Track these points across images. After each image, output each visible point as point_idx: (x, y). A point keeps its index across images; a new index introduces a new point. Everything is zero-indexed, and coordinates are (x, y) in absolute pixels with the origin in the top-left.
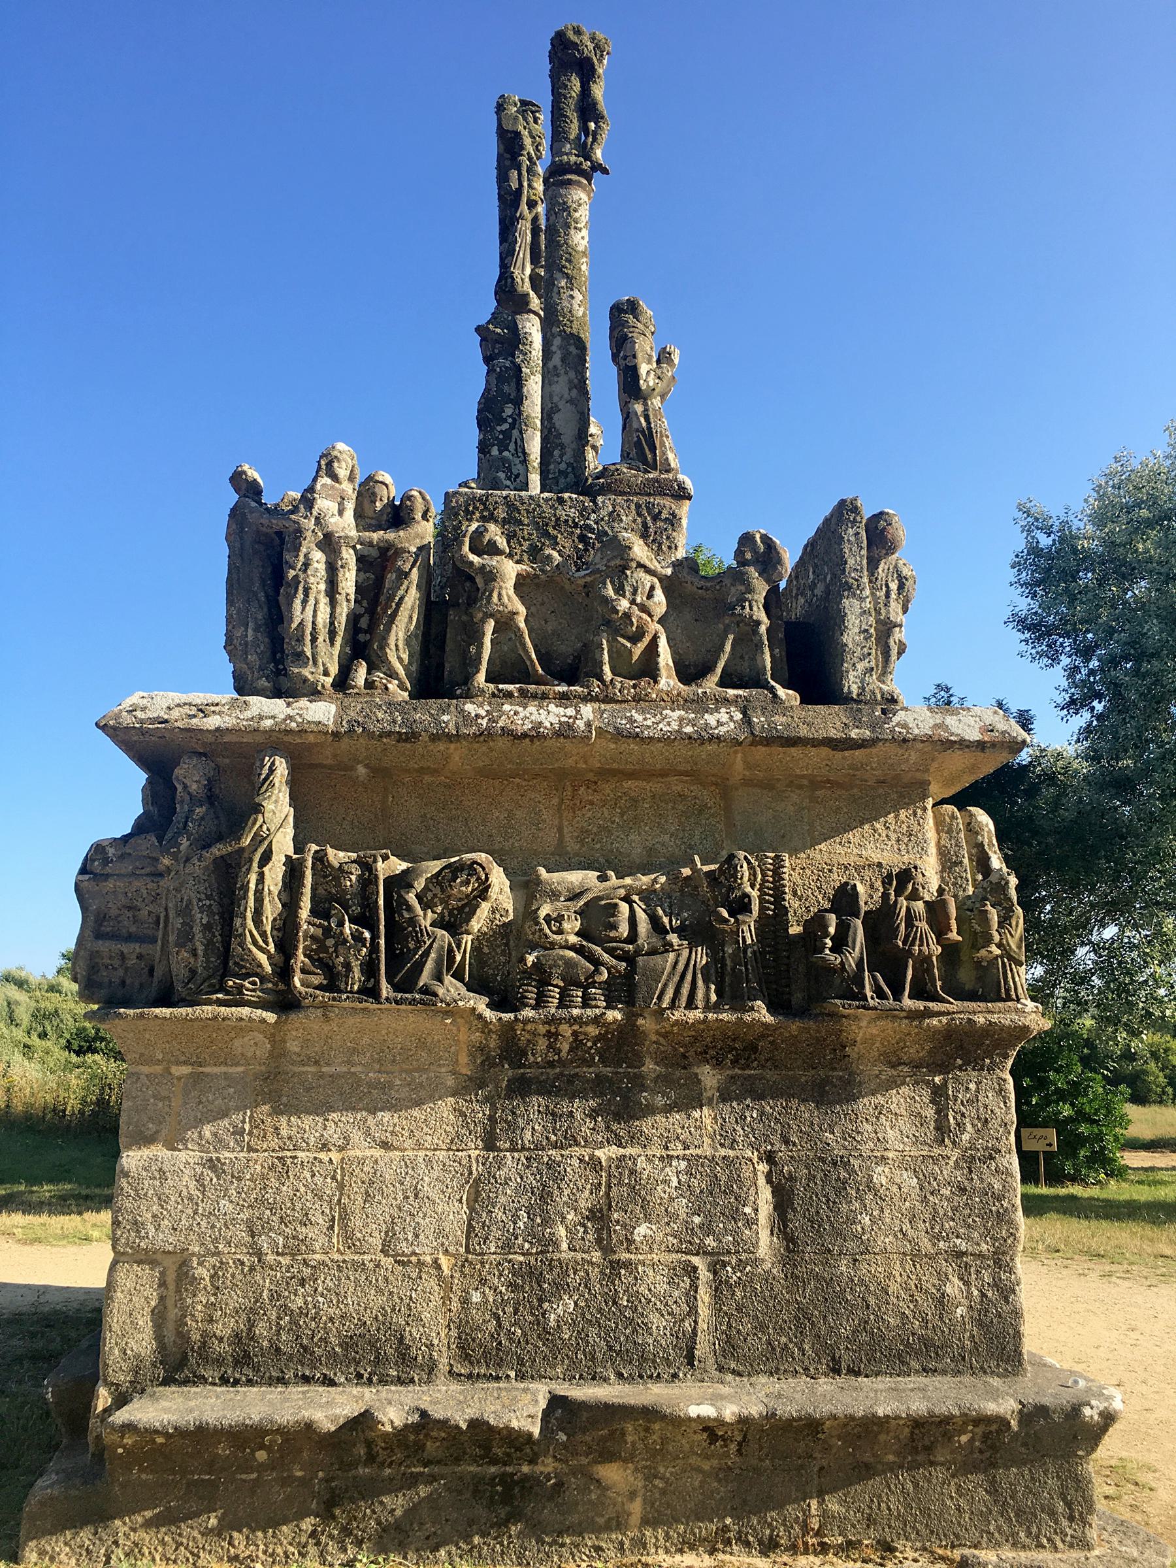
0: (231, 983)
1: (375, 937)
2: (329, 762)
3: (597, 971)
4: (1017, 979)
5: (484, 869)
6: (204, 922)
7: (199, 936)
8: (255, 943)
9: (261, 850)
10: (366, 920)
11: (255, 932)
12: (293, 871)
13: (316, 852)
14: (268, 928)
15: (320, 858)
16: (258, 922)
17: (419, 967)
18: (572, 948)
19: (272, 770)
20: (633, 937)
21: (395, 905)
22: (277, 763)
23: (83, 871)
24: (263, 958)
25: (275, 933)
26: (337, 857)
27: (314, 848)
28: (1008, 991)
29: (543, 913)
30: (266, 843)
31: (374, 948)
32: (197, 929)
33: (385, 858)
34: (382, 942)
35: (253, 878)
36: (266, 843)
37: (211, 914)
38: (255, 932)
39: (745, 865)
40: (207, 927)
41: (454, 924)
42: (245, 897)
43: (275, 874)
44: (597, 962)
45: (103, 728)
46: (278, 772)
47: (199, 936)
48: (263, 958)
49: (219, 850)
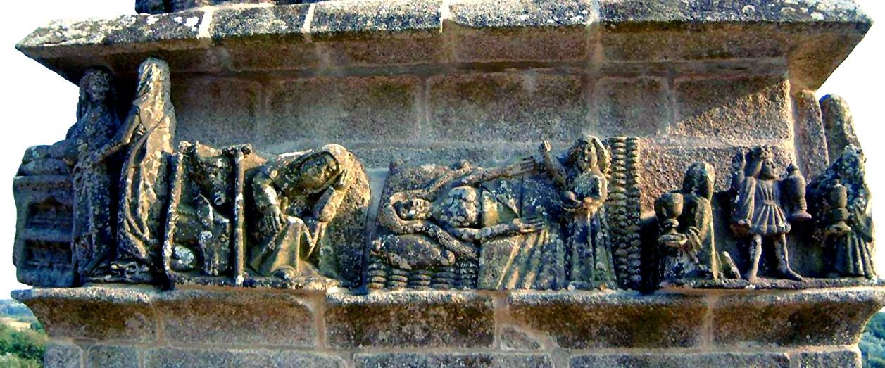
0: (114, 267)
1: (234, 224)
2: (214, 69)
3: (445, 255)
4: (866, 255)
5: (335, 159)
6: (96, 213)
7: (92, 225)
8: (133, 231)
9: (138, 147)
10: (226, 209)
11: (132, 220)
12: (169, 165)
13: (189, 148)
14: (145, 218)
15: (191, 154)
16: (134, 212)
17: (272, 254)
18: (423, 233)
19: (149, 76)
20: (479, 223)
21: (252, 192)
22: (154, 69)
23: (20, 173)
24: (140, 246)
25: (152, 222)
26: (206, 152)
27: (185, 144)
28: (856, 268)
29: (393, 199)
30: (142, 141)
31: (233, 236)
32: (91, 220)
33: (246, 152)
34: (240, 230)
35: (131, 172)
36: (142, 141)
37: (103, 206)
38: (132, 220)
39: (593, 149)
40: (99, 218)
41: (310, 212)
42: (124, 191)
43: (152, 168)
44: (444, 248)
45: (20, 48)
46: (154, 78)
47: (92, 225)
48: (140, 246)
49: (107, 149)
